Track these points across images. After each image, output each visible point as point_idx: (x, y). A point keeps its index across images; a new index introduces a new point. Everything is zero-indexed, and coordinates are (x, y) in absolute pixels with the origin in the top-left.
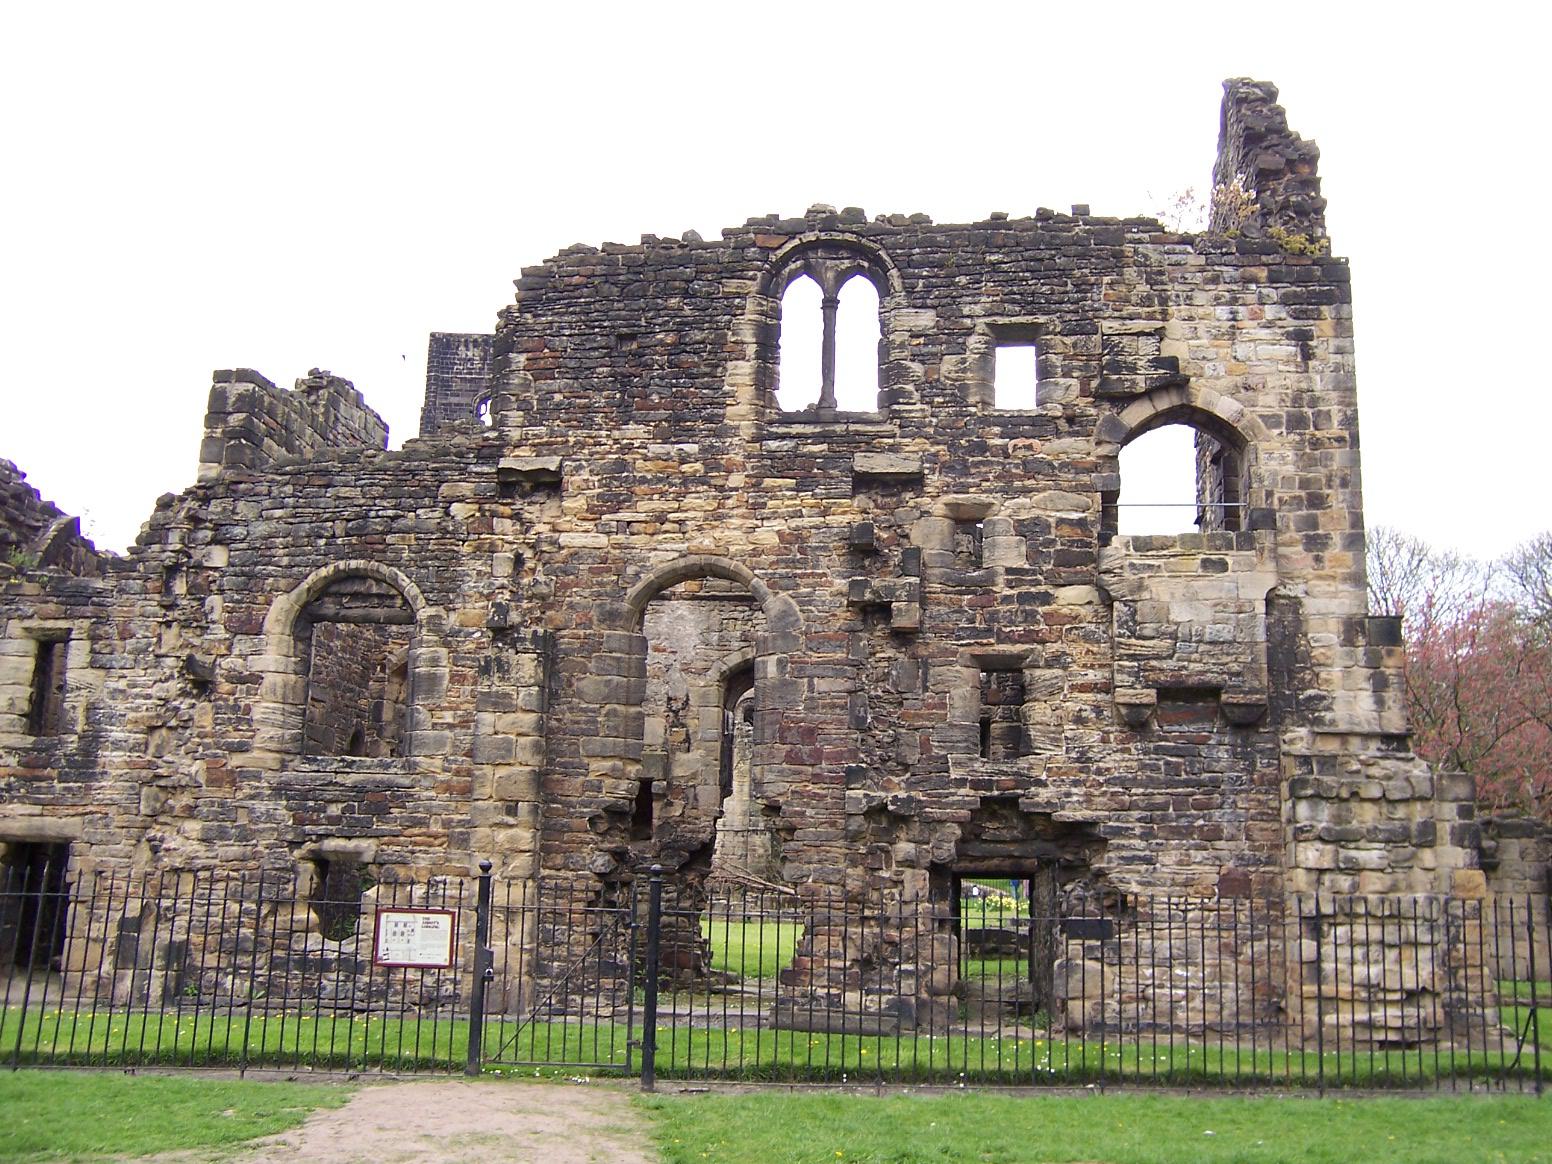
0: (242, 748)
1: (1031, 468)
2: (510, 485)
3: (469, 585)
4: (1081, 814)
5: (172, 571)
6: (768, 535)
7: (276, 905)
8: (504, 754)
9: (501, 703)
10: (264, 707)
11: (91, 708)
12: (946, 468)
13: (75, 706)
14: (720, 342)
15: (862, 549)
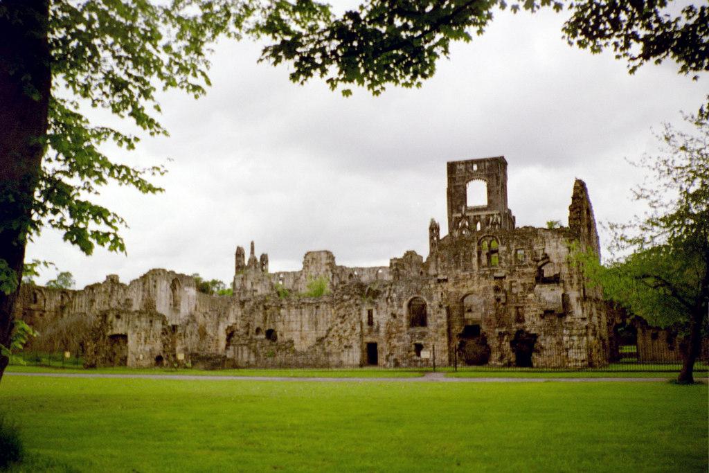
0: (401, 327)
1: (524, 274)
2: (439, 281)
3: (434, 298)
4: (534, 332)
5: (387, 299)
6: (482, 287)
7: (409, 352)
8: (442, 326)
9: (441, 318)
10: (404, 320)
11: (378, 322)
12: (509, 275)
13: (375, 321)
14: (471, 254)
15: (497, 289)
